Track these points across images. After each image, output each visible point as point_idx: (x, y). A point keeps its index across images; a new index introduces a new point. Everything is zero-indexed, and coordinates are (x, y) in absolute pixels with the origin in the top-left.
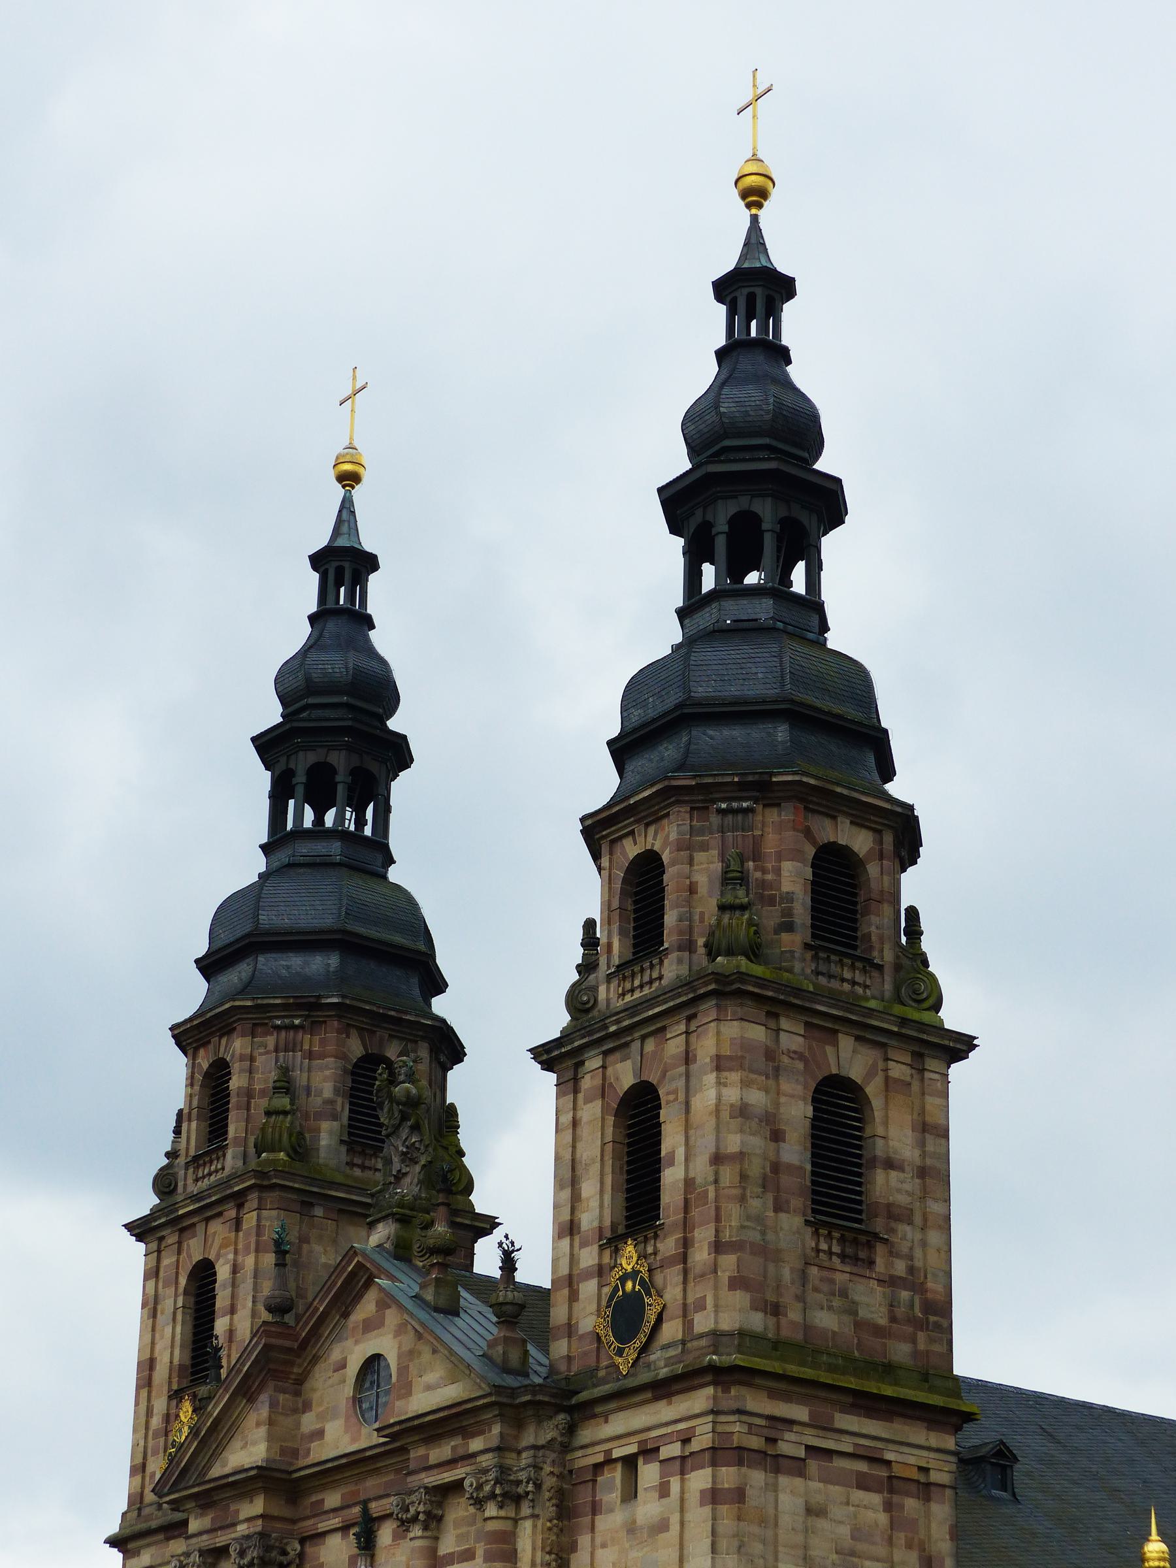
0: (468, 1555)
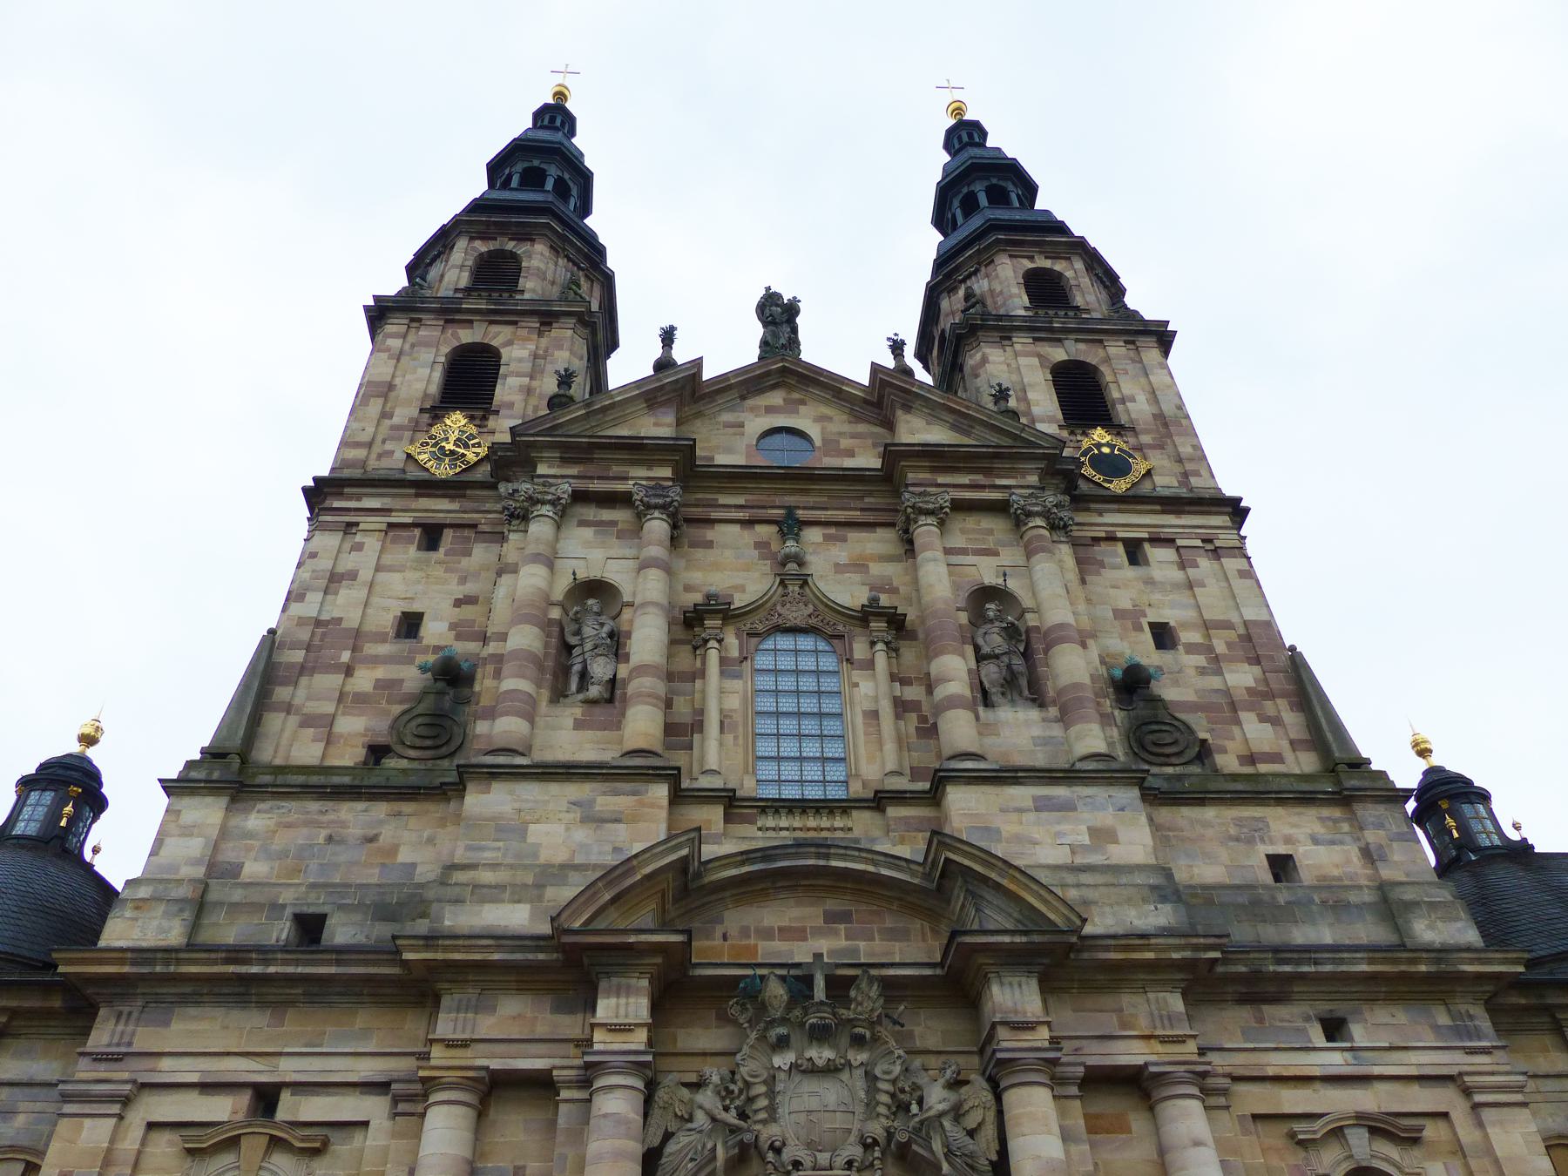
0: (993, 553)
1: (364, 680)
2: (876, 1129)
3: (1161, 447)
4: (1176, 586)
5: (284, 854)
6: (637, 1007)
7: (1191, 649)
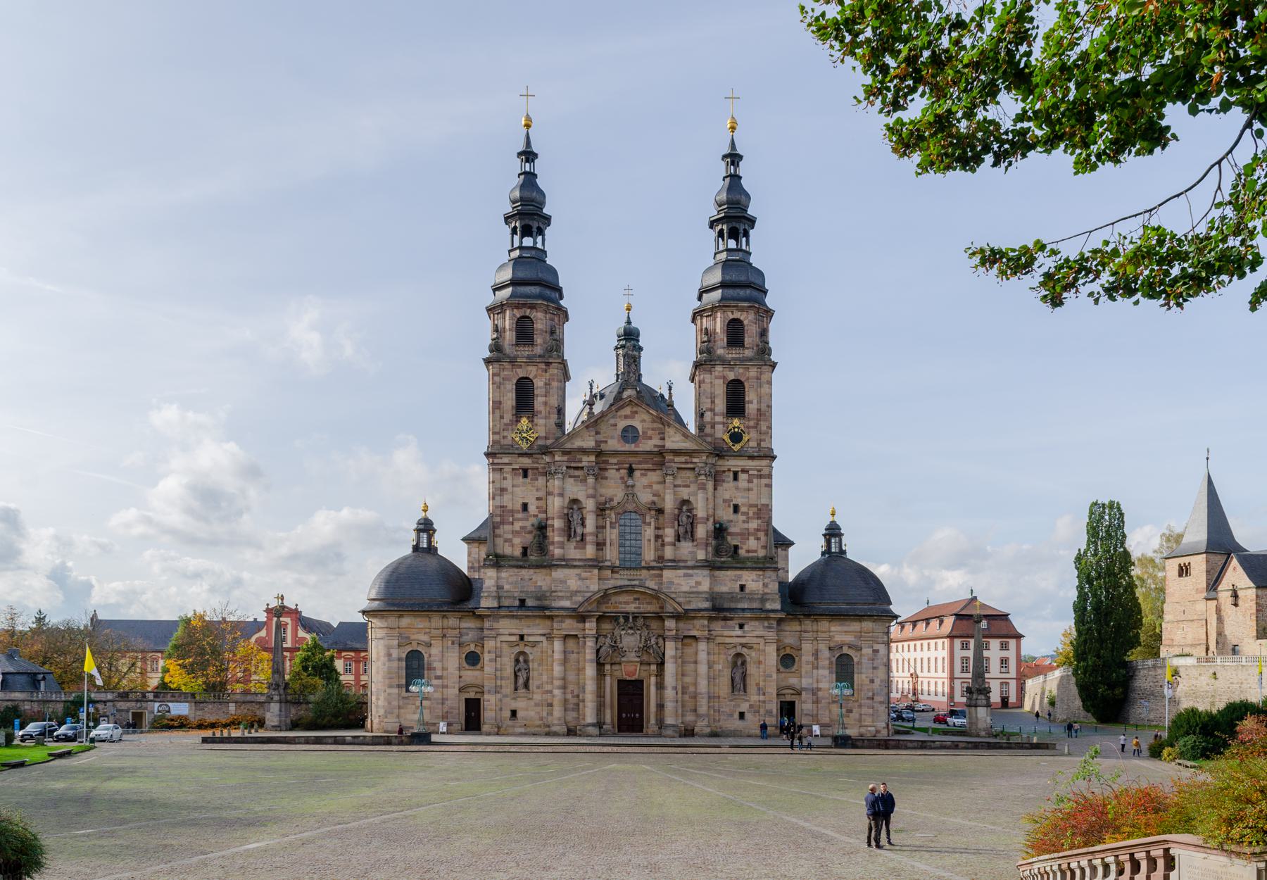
0: (688, 486)
1: (517, 526)
2: (641, 645)
3: (756, 427)
4: (745, 490)
5: (512, 583)
6: (594, 624)
7: (744, 514)
